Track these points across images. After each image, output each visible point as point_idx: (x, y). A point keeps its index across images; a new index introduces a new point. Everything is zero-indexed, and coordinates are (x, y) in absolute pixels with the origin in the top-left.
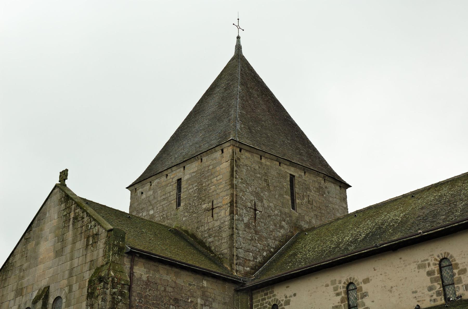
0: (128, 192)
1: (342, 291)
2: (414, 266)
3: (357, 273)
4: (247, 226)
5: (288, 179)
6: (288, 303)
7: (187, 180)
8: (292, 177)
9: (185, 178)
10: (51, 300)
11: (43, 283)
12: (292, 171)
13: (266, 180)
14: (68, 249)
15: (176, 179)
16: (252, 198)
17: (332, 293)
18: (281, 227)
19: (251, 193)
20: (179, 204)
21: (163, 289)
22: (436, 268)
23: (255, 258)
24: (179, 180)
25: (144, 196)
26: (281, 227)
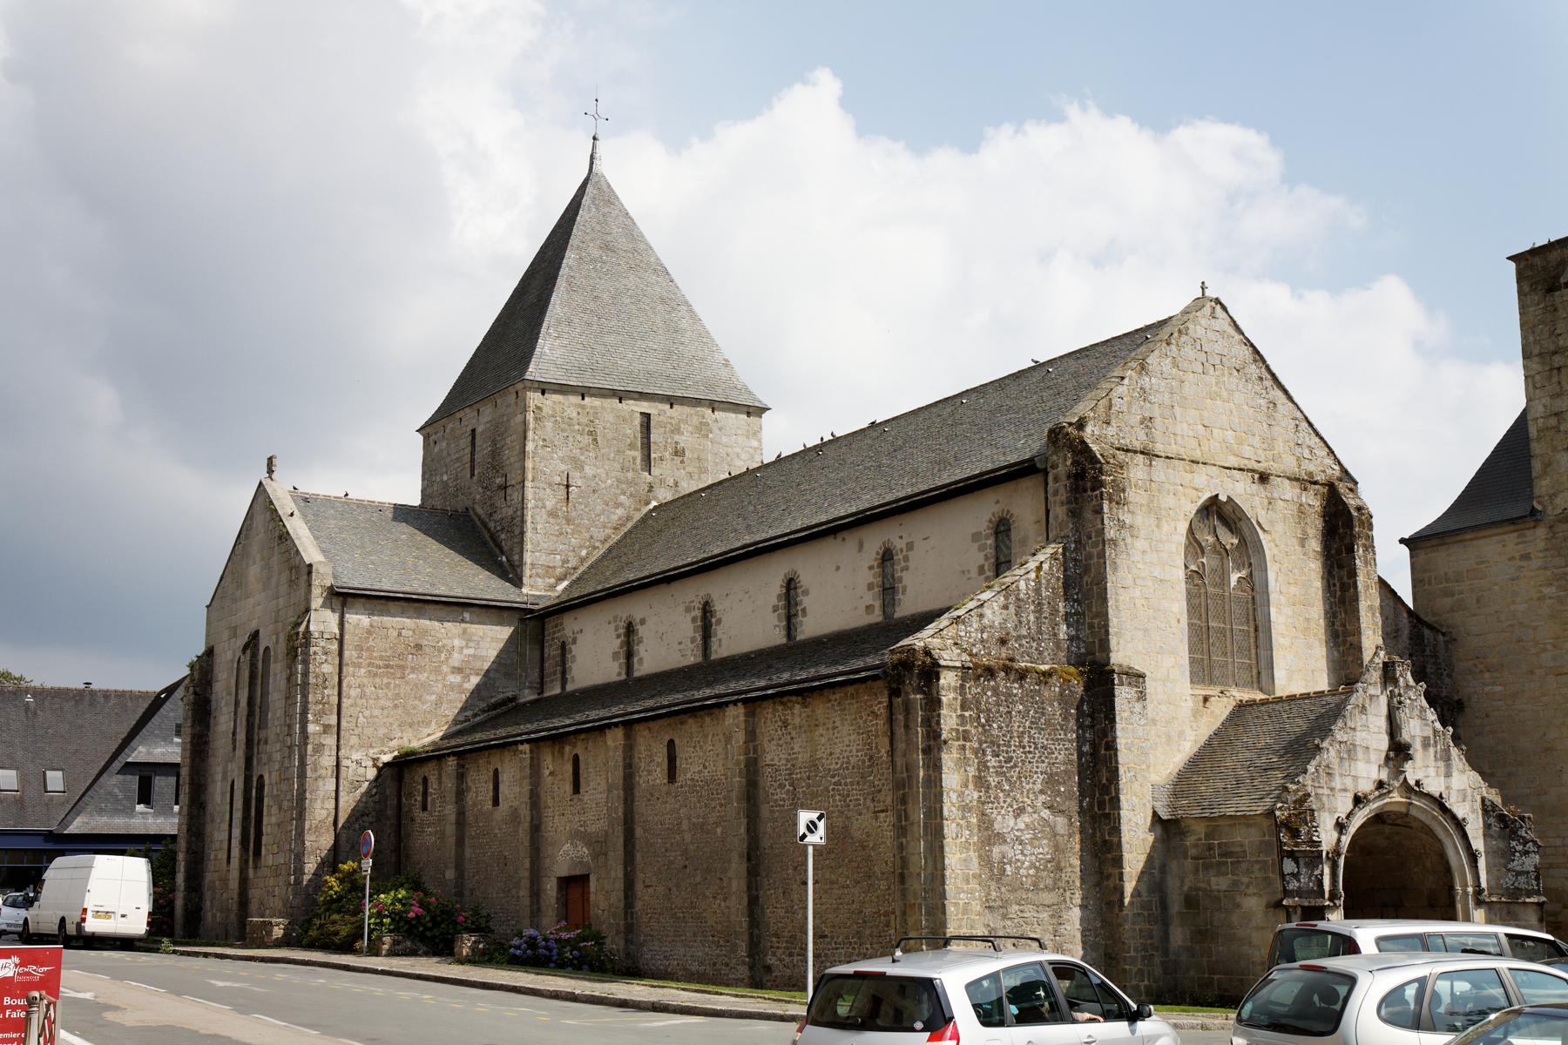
0: (420, 438)
1: (622, 631)
2: (682, 608)
3: (635, 608)
4: (553, 514)
5: (637, 420)
6: (574, 641)
7: (483, 433)
8: (647, 417)
9: (479, 430)
10: (261, 652)
11: (253, 626)
12: (645, 407)
13: (590, 433)
14: (274, 580)
15: (469, 429)
16: (563, 467)
17: (614, 635)
18: (618, 505)
19: (562, 460)
20: (472, 475)
21: (395, 634)
22: (698, 613)
23: (565, 561)
24: (473, 431)
25: (437, 449)
26: (618, 505)
